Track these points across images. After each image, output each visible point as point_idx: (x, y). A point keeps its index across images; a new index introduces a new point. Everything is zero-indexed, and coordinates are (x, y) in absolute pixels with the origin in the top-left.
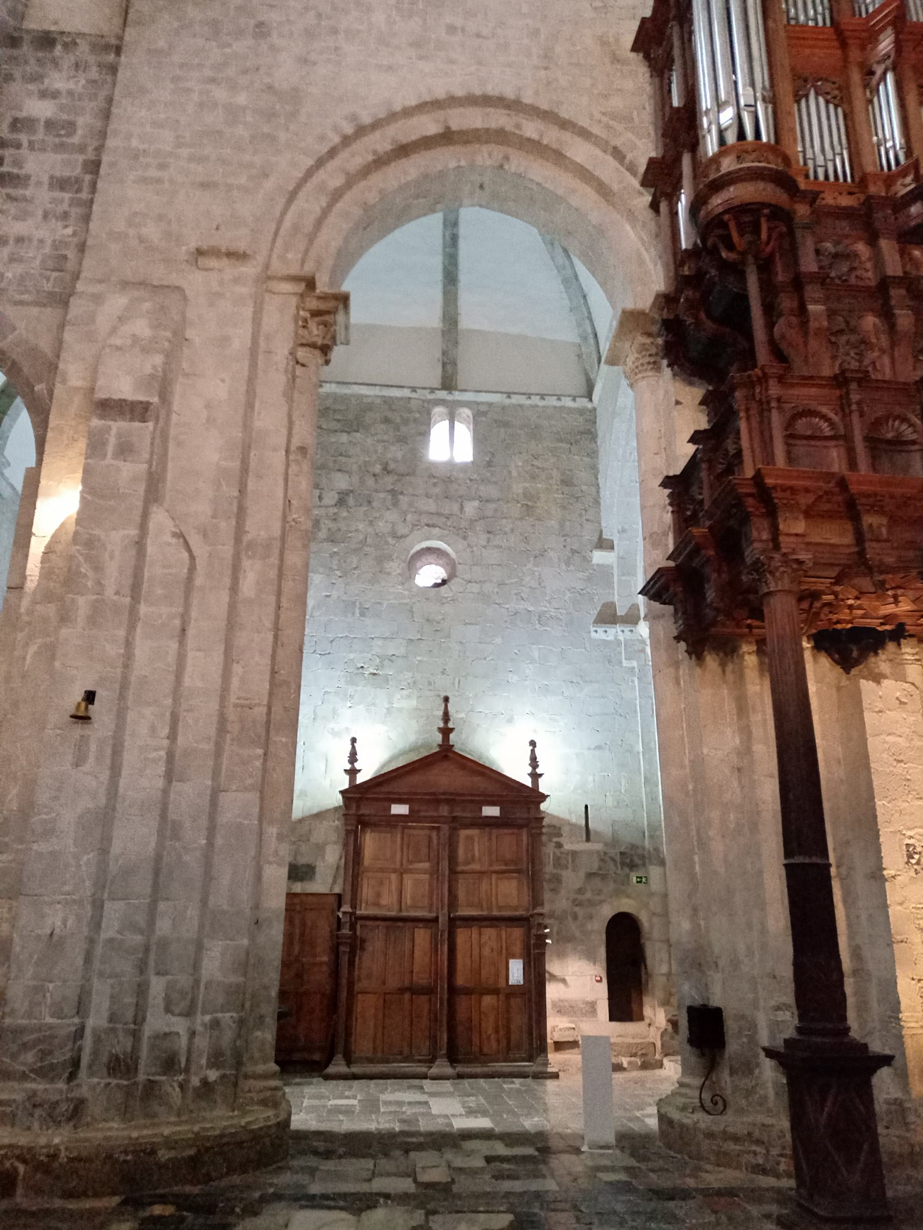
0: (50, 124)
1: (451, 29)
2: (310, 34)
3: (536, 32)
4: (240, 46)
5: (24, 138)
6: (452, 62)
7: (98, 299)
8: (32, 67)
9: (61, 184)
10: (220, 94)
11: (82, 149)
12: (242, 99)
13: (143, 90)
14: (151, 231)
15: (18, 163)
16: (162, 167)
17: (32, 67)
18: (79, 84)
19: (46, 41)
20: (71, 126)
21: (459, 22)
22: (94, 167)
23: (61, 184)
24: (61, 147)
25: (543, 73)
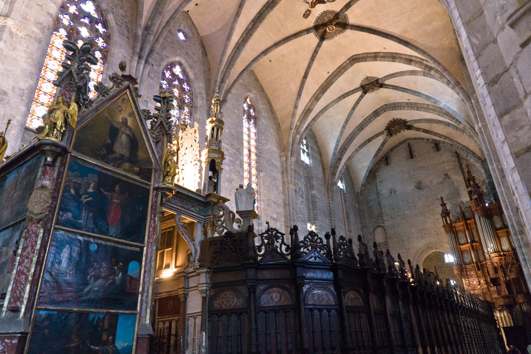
1: (425, 234)
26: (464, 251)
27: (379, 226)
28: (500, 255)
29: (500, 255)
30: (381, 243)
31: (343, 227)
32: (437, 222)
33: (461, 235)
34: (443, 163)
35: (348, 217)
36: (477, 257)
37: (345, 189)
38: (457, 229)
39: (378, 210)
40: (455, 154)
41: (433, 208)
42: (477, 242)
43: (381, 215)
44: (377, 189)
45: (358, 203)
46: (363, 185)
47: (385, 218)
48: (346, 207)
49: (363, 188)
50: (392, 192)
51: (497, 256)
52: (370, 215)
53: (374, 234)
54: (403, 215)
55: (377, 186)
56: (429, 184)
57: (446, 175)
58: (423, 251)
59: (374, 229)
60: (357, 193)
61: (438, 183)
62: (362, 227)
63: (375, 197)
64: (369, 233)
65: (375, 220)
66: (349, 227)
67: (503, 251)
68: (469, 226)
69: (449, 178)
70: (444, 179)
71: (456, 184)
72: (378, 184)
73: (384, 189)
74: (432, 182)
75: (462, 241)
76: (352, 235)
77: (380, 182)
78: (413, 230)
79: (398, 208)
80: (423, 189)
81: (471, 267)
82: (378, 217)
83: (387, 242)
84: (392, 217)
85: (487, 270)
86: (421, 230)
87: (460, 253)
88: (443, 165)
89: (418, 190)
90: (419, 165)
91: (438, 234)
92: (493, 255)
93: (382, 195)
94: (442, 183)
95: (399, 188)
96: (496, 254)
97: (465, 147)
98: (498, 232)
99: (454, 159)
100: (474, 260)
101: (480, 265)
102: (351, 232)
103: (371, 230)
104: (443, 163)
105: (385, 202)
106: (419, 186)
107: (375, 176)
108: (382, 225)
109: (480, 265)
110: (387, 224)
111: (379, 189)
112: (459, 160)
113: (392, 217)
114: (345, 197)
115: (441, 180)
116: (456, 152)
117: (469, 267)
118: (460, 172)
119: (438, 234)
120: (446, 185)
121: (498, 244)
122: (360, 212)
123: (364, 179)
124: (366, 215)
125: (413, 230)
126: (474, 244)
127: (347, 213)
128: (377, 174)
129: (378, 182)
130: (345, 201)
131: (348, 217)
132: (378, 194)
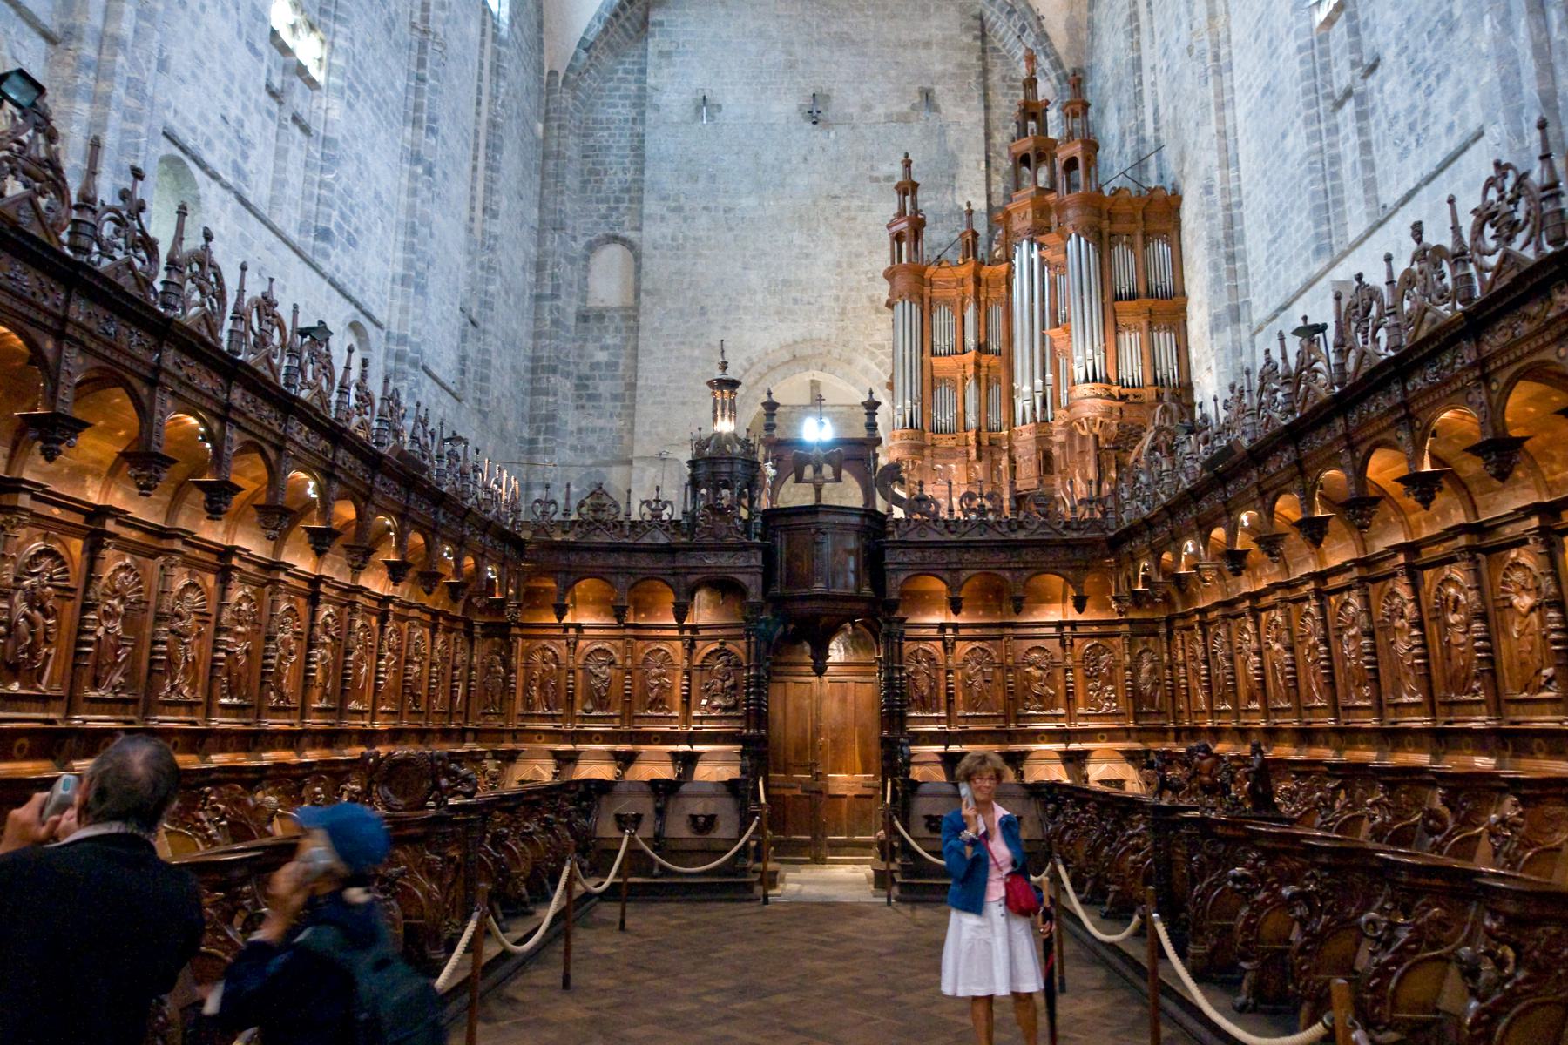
0: (608, 365)
1: (795, 301)
2: (727, 311)
3: (837, 299)
4: (693, 321)
5: (596, 373)
6: (795, 321)
7: (643, 470)
8: (596, 333)
9: (615, 398)
10: (686, 351)
11: (623, 378)
12: (697, 353)
13: (651, 353)
14: (661, 429)
15: (595, 388)
16: (664, 394)
17: (596, 333)
18: (617, 341)
19: (600, 317)
20: (616, 364)
21: (798, 295)
22: (632, 386)
23: (615, 398)
24: (613, 378)
25: (840, 324)
26: (942, 380)
27: (615, 239)
28: (1111, 396)
29: (1111, 396)
30: (607, 309)
31: (467, 167)
32: (850, 266)
33: (944, 319)
34: (927, 45)
35: (494, 147)
36: (984, 408)
38: (937, 293)
40: (977, 23)
41: (849, 208)
42: (998, 353)
43: (635, 192)
44: (641, 82)
45: (547, 120)
46: (586, 46)
47: (651, 206)
48: (494, 97)
49: (583, 55)
50: (704, 105)
51: (1097, 396)
52: (585, 182)
53: (586, 268)
55: (643, 71)
56: (854, 111)
57: (927, 95)
58: (771, 368)
59: (591, 247)
60: (553, 73)
61: (889, 118)
62: (542, 221)
63: (626, 112)
64: (566, 257)
65: (603, 207)
66: (490, 190)
67: (1120, 382)
68: (983, 289)
69: (936, 109)
70: (913, 107)
71: (952, 133)
72: (652, 58)
73: (672, 89)
74: (867, 108)
75: (943, 341)
76: (496, 230)
77: (663, 54)
78: (754, 278)
79: (712, 178)
80: (828, 125)
81: (952, 443)
82: (618, 200)
83: (636, 308)
84: (678, 210)
85: (1012, 460)
86: (785, 282)
87: (927, 385)
88: (923, 53)
89: (809, 125)
90: (834, 28)
91: (843, 312)
92: (1084, 390)
93: (657, 108)
94: (904, 119)
95: (734, 99)
96: (1098, 388)
98: (1118, 305)
99: (967, 39)
100: (971, 420)
101: (985, 442)
102: (495, 216)
103: (579, 246)
105: (659, 142)
106: (816, 113)
107: (645, 23)
108: (631, 235)
109: (985, 442)
110: (652, 233)
111: (651, 81)
112: (984, 51)
113: (678, 210)
114: (498, 55)
115: (906, 108)
116: (980, 17)
117: (946, 441)
118: (977, 94)
119: (843, 312)
120: (916, 132)
121: (1111, 355)
122: (545, 157)
123: (599, 17)
124: (572, 181)
125: (754, 278)
126: (984, 359)
127: (493, 125)
128: (655, 16)
129: (651, 48)
130: (497, 71)
131: (494, 147)
132: (641, 100)
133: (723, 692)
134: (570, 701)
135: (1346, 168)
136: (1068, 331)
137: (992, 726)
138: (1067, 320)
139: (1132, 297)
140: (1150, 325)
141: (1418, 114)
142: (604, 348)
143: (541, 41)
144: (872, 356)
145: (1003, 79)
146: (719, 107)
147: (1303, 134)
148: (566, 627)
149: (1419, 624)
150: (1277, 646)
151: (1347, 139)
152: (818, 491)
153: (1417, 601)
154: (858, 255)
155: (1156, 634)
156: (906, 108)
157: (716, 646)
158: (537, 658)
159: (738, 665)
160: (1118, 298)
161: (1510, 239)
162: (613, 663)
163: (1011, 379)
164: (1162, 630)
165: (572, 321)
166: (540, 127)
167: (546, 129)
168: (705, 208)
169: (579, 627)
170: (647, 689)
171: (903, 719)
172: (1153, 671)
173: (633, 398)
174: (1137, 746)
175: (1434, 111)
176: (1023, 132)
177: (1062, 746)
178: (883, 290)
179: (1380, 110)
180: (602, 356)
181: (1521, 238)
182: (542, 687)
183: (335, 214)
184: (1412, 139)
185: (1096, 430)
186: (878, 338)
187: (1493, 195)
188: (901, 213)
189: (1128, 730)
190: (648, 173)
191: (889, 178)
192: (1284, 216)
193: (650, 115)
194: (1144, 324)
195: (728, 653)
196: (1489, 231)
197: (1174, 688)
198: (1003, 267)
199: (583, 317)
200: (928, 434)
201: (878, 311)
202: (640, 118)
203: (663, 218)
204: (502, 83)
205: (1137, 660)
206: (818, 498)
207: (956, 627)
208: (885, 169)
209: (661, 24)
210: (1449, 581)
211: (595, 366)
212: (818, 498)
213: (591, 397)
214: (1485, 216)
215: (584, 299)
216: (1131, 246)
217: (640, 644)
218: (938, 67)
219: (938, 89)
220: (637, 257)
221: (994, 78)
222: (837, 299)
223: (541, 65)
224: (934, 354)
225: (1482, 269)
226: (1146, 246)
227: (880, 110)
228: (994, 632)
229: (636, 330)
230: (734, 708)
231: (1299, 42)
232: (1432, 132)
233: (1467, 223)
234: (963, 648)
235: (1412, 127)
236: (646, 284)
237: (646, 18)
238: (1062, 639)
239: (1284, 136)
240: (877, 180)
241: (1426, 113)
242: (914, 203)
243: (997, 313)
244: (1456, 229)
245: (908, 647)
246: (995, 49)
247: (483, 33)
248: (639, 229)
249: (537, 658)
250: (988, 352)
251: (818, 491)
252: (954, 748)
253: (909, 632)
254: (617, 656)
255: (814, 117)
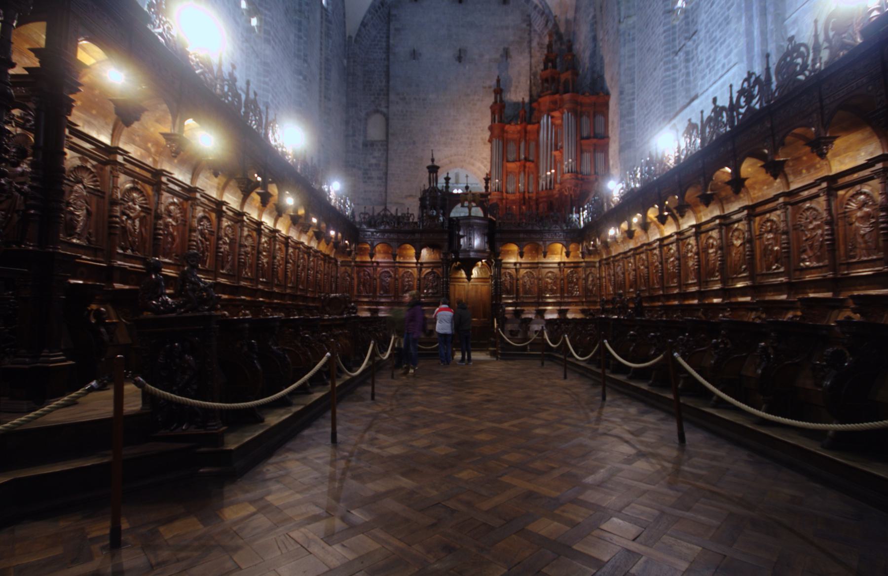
0: (376, 165)
1: (452, 139)
22: (386, 174)
27: (377, 111)
32: (474, 124)
33: (512, 147)
34: (507, 28)
37: (330, 8)
39: (381, 82)
42: (533, 162)
44: (388, 42)
47: (392, 97)
54: (424, 100)
59: (368, 115)
60: (350, 37)
67: (581, 173)
69: (510, 57)
72: (392, 31)
74: (481, 56)
75: (511, 157)
82: (379, 94)
91: (471, 144)
92: (567, 176)
97: (548, 7)
98: (582, 142)
99: (524, 26)
104: (507, 28)
108: (384, 110)
111: (391, 41)
116: (529, 16)
118: (527, 51)
119: (471, 144)
126: (528, 164)
133: (432, 288)
134: (375, 292)
135: (678, 83)
136: (562, 153)
137: (533, 300)
138: (562, 147)
139: (588, 138)
140: (595, 150)
141: (711, 59)
142: (374, 157)
143: (345, 22)
144: (482, 163)
145: (538, 44)
146: (420, 54)
147: (663, 68)
148: (373, 262)
149: (697, 254)
150: (642, 267)
151: (680, 70)
152: (470, 210)
153: (697, 245)
154: (477, 120)
155: (594, 267)
156: (498, 56)
157: (429, 270)
158: (362, 274)
159: (438, 277)
160: (582, 138)
161: (751, 102)
162: (390, 276)
163: (538, 172)
164: (597, 265)
165: (361, 146)
166: (345, 61)
167: (348, 62)
168: (415, 99)
169: (378, 263)
170: (404, 286)
171: (501, 299)
172: (593, 281)
173: (386, 179)
174: (586, 307)
175: (718, 58)
176: (546, 68)
177: (558, 308)
178: (487, 135)
179: (695, 59)
180: (373, 161)
181: (755, 101)
182: (364, 286)
183: (270, 96)
184: (707, 71)
185: (572, 192)
186: (484, 155)
187: (746, 85)
188: (495, 102)
189: (583, 302)
190: (391, 83)
191: (490, 87)
192: (652, 104)
193: (391, 57)
194: (592, 149)
195: (434, 273)
196: (743, 99)
197: (601, 286)
198: (536, 126)
199: (365, 145)
200: (505, 194)
201: (485, 144)
202: (388, 59)
203: (397, 103)
204: (330, 41)
205: (587, 276)
206: (470, 213)
207: (520, 263)
208: (488, 83)
209: (395, 16)
210: (711, 237)
211: (371, 165)
212: (470, 213)
213: (369, 178)
214: (741, 92)
215: (365, 137)
216: (588, 116)
217: (401, 269)
218: (511, 38)
219: (511, 48)
220: (387, 120)
221: (534, 44)
222: (468, 138)
223: (345, 33)
224: (508, 161)
225: (739, 114)
226: (594, 116)
227: (487, 57)
228: (535, 266)
229: (387, 150)
230: (437, 293)
231: (665, 28)
232: (716, 68)
233: (735, 96)
234: (523, 272)
235: (708, 66)
236: (391, 131)
237: (389, 13)
238: (560, 268)
239: (655, 69)
240: (484, 87)
241: (714, 60)
242: (501, 98)
243: (532, 145)
244: (731, 98)
245: (503, 271)
246: (535, 31)
247: (322, 17)
248: (388, 107)
249: (362, 274)
250: (529, 161)
251: (470, 210)
252: (518, 308)
253: (504, 265)
254: (392, 273)
255: (459, 59)
